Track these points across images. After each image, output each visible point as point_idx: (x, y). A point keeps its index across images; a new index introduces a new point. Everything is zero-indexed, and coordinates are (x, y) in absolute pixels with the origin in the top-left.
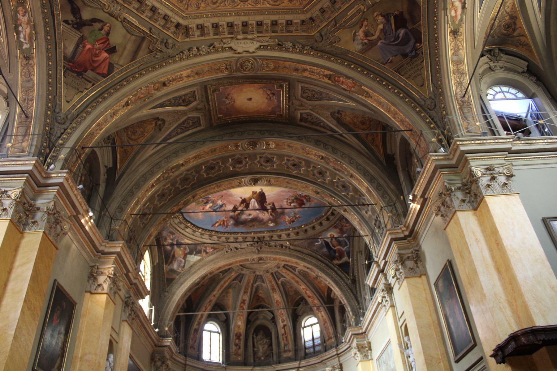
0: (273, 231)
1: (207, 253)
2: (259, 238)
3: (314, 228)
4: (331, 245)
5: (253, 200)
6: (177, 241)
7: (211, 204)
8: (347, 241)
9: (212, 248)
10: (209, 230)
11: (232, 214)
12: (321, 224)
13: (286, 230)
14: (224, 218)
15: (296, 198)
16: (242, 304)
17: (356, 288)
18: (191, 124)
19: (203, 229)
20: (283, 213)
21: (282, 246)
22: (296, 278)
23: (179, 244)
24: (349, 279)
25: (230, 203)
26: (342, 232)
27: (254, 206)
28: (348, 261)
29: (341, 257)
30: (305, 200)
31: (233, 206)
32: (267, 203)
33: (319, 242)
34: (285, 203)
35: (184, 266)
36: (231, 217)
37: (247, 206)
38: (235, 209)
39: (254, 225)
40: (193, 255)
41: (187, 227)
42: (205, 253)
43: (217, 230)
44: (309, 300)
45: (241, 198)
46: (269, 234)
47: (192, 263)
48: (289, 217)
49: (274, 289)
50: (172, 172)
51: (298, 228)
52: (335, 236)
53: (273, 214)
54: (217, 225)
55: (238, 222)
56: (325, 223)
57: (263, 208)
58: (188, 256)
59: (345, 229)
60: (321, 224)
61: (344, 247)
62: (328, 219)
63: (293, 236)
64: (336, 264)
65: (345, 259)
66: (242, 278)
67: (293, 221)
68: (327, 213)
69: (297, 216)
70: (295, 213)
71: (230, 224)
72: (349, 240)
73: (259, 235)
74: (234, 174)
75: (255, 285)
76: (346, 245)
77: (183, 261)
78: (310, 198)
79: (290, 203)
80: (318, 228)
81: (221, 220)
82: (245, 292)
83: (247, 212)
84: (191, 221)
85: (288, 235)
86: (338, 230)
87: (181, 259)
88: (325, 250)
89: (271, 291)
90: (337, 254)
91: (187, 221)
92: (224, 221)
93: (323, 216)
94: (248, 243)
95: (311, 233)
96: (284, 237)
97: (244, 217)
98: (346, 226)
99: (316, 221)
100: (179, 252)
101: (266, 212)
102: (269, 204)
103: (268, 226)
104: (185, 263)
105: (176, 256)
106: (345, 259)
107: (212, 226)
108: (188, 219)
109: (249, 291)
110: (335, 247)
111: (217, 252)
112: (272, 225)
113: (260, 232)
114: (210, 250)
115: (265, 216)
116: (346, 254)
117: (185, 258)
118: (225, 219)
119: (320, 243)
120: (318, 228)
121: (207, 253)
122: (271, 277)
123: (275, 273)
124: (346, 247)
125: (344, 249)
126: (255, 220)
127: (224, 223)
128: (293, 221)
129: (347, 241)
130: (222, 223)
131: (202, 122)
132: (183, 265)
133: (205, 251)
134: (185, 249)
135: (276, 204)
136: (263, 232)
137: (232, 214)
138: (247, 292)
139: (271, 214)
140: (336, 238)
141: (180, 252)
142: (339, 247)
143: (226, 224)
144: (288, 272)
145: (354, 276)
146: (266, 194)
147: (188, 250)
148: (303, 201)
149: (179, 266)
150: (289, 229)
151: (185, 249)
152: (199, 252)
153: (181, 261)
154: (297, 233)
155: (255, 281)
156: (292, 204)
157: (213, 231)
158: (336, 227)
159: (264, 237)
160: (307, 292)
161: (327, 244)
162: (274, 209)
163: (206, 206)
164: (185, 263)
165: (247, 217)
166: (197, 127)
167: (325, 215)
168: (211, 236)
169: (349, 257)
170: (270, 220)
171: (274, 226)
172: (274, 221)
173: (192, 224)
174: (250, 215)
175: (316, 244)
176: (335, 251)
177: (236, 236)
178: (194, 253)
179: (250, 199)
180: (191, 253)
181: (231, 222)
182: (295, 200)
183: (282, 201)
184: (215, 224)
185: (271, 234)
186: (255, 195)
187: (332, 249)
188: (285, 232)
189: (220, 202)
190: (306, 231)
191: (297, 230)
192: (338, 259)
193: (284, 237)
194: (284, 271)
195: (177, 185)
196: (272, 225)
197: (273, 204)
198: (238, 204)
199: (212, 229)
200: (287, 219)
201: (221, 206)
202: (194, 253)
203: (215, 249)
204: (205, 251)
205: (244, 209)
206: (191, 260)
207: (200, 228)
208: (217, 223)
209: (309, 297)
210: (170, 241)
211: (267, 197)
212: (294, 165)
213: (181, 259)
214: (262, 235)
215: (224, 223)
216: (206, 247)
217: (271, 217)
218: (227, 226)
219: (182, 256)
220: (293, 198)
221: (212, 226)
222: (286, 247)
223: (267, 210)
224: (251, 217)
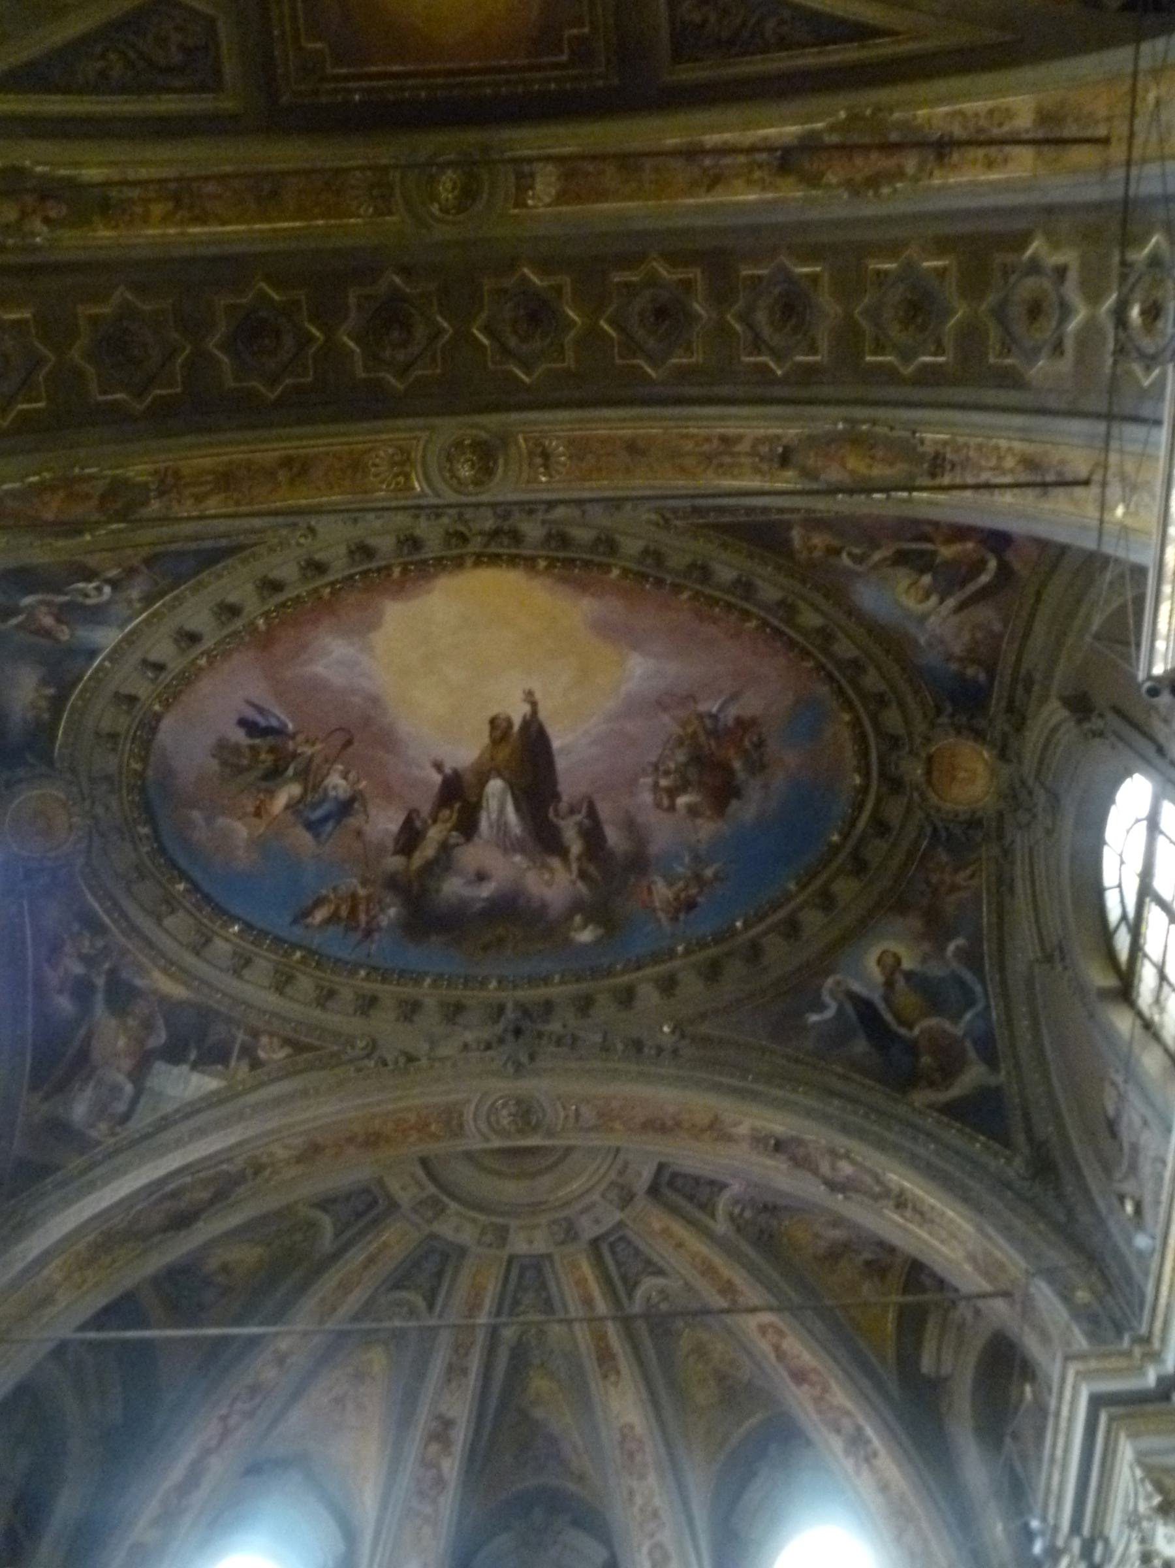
0: (596, 973)
1: (256, 1064)
2: (525, 1011)
3: (792, 929)
4: (888, 1017)
5: (495, 785)
6: (113, 973)
7: (295, 789)
8: (968, 976)
9: (287, 1042)
10: (278, 940)
11: (394, 863)
12: (827, 900)
13: (656, 958)
14: (352, 883)
15: (698, 759)
16: (434, 1448)
17: (1060, 1197)
18: (177, 58)
19: (248, 927)
20: (638, 863)
21: (637, 1046)
22: (719, 1261)
23: (121, 996)
24: (1009, 1161)
25: (388, 793)
26: (936, 928)
27: (501, 826)
28: (993, 1081)
29: (948, 1070)
30: (737, 765)
31: (401, 818)
32: (563, 806)
33: (820, 1007)
34: (647, 797)
35: (125, 1118)
36: (393, 883)
37: (468, 826)
38: (409, 838)
39: (501, 941)
40: (185, 1068)
41: (171, 903)
42: (244, 1067)
43: (317, 940)
44: (799, 1401)
45: (438, 766)
46: (572, 988)
47: (169, 1108)
48: (670, 884)
49: (605, 1357)
50: (47, 220)
51: (718, 939)
52: (907, 965)
53: (591, 869)
54: (320, 915)
55: (426, 918)
56: (845, 888)
57: (544, 839)
58: (160, 1066)
59: (950, 904)
60: (827, 900)
61: (956, 1018)
62: (859, 866)
63: (691, 985)
64: (931, 1106)
65: (974, 1075)
66: (439, 1275)
67: (691, 905)
68: (853, 823)
69: (709, 873)
70: (696, 858)
71: (384, 920)
72: (978, 970)
73: (526, 994)
74: (371, 404)
75: (509, 1334)
76: (970, 1004)
77: (129, 1088)
78: (760, 745)
79: (673, 793)
80: (812, 919)
81: (343, 889)
82: (455, 1371)
83: (472, 856)
84: (197, 874)
85: (668, 985)
86: (916, 923)
87: (121, 1078)
88: (861, 1046)
89: (590, 1364)
90: (926, 1060)
91: (174, 865)
92: (354, 896)
93: (835, 849)
94: (469, 1036)
95: (780, 956)
96: (649, 996)
97: (453, 887)
98: (955, 888)
99: (803, 887)
100: (113, 1038)
101: (555, 862)
102: (572, 811)
103: (568, 941)
104: (134, 1101)
105: (96, 1056)
106: (974, 1075)
107: (295, 921)
108: (183, 862)
109: (475, 1363)
110: (910, 1027)
111: (310, 1068)
112: (586, 936)
113: (533, 981)
114: (273, 1053)
115: (554, 885)
116: (972, 1054)
117: (139, 1074)
118: (362, 892)
119: (829, 1014)
120: (812, 919)
121: (256, 1064)
122: (586, 1268)
123: (612, 1246)
124: (968, 1016)
125: (958, 1030)
126: (509, 913)
127: (353, 911)
128: (691, 905)
129: (968, 976)
130: (344, 912)
131: (230, 68)
132: (121, 1107)
133: (248, 1052)
134: (148, 1025)
135: (605, 810)
136: (546, 980)
137: (394, 863)
138: (465, 1372)
139: (583, 875)
140: (909, 976)
141: (121, 1043)
142: (932, 1022)
143: (363, 918)
144: (679, 1229)
145: (1039, 1147)
146: (556, 744)
147: (160, 1038)
148: (725, 768)
149: (100, 1110)
150: (671, 954)
151: (148, 1025)
152: (214, 1056)
153: (116, 1089)
154: (712, 972)
155: (508, 1304)
156: (682, 800)
157: (295, 946)
158: (902, 907)
159: (548, 1007)
160: (785, 1345)
161: (866, 1011)
162: (593, 835)
163: (271, 793)
164: (134, 1101)
165: (467, 892)
166: (202, 88)
167: (845, 837)
168: (283, 982)
169: (992, 1062)
170: (577, 906)
171: (597, 942)
172: (597, 911)
173: (195, 887)
174: (481, 877)
175: (814, 1018)
176: (912, 1048)
177: (409, 991)
178: (193, 1056)
179: (482, 782)
180: (174, 1053)
181: (392, 912)
182: (692, 774)
183: (632, 784)
184: (307, 913)
185: (584, 987)
186: (504, 753)
187: (896, 1037)
188: (649, 971)
189: (337, 783)
190: (755, 951)
191: (712, 951)
192: (932, 1084)
193: (649, 996)
194: (658, 1219)
195: (75, 355)
196: (586, 936)
197: (592, 813)
198: (426, 809)
199: (297, 933)
200: (662, 891)
201: (346, 808)
202: (193, 1056)
203: (299, 1048)
204: (248, 1052)
205: (455, 837)
206: (171, 1091)
207: (235, 919)
208: (319, 902)
209: (799, 1376)
210: (78, 969)
211: (561, 764)
212: (661, 313)
213: (121, 1078)
214: (542, 992)
215: (353, 911)
216: (255, 1034)
217: (580, 885)
218: (368, 933)
219: (127, 1064)
220: (681, 756)
221: (295, 921)
222: (660, 1050)
223: (562, 851)
224: (486, 891)
